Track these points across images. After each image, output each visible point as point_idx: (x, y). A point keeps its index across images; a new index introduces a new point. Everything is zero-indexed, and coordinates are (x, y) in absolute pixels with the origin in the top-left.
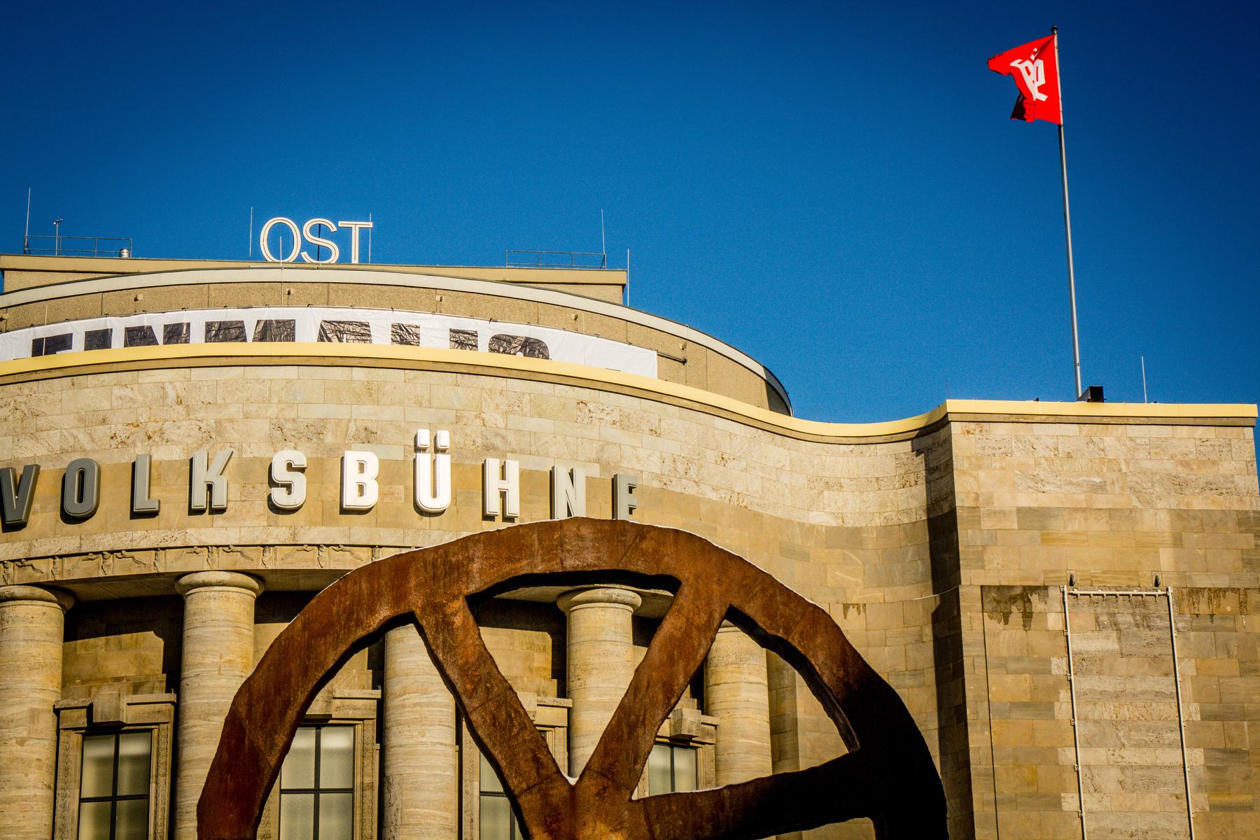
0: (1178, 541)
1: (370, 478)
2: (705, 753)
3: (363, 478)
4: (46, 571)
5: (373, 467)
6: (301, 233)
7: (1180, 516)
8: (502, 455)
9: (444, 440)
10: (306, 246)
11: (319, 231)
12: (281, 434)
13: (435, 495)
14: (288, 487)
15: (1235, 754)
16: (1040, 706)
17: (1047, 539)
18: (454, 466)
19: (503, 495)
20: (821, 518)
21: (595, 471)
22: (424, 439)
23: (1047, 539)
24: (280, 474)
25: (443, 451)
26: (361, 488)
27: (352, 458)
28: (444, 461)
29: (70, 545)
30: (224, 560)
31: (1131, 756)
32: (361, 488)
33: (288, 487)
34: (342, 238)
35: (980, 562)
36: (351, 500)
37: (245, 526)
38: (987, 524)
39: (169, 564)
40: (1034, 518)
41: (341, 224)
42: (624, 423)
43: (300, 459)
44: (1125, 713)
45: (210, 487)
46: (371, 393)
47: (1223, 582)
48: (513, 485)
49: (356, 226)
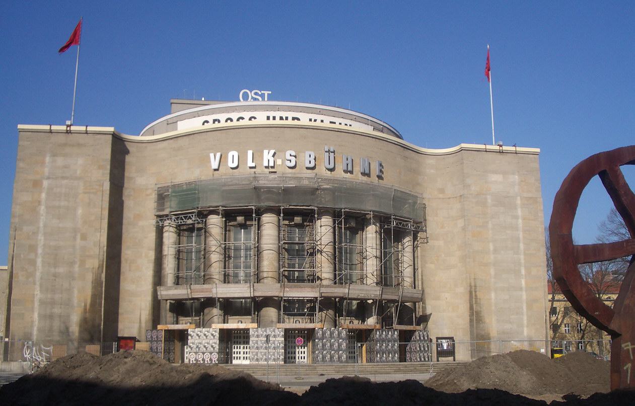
1: (312, 159)
6: (251, 94)
10: (252, 98)
11: (256, 94)
13: (329, 164)
14: (290, 161)
34: (262, 96)
41: (262, 92)
43: (293, 153)
45: (269, 160)
49: (266, 93)
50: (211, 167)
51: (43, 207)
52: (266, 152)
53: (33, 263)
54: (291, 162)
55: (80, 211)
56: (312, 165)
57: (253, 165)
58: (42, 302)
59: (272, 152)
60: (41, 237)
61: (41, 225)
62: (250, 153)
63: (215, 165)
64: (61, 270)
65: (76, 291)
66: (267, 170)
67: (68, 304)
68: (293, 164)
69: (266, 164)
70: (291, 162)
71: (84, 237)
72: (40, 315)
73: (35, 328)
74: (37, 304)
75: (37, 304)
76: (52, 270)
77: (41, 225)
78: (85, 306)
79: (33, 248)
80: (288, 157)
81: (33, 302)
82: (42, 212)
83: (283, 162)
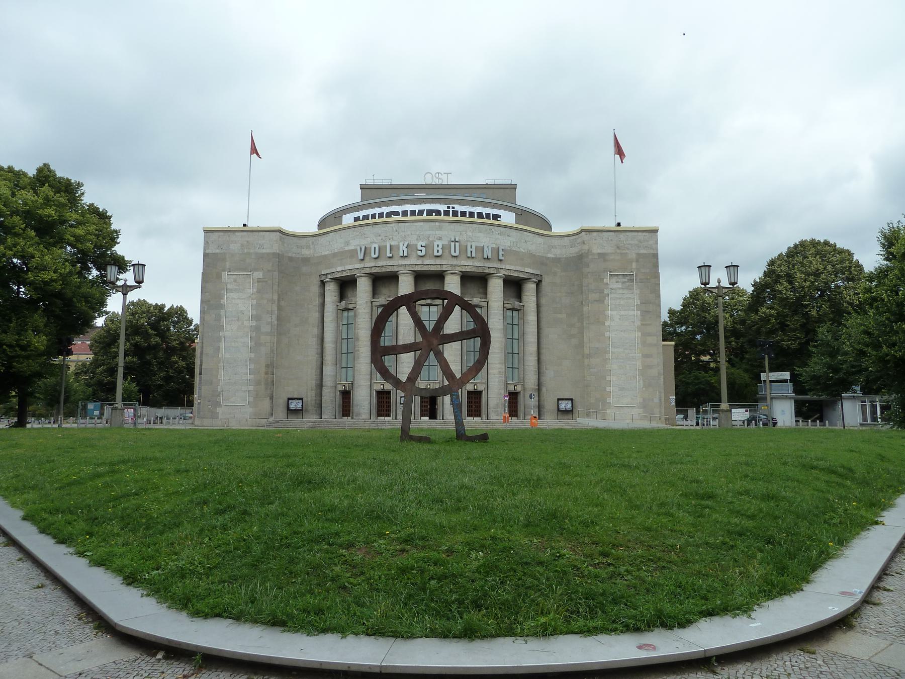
0: (637, 261)
2: (521, 312)
4: (368, 271)
5: (440, 246)
7: (638, 254)
12: (419, 238)
15: (648, 312)
16: (601, 301)
17: (605, 260)
20: (549, 255)
21: (494, 246)
23: (605, 260)
29: (372, 264)
30: (408, 268)
31: (623, 312)
35: (588, 266)
36: (436, 254)
37: (412, 261)
38: (590, 257)
39: (396, 269)
40: (602, 256)
42: (501, 234)
44: (622, 302)
46: (440, 228)
47: (648, 271)
48: (474, 250)
56: (439, 254)
68: (423, 253)
80: (420, 248)
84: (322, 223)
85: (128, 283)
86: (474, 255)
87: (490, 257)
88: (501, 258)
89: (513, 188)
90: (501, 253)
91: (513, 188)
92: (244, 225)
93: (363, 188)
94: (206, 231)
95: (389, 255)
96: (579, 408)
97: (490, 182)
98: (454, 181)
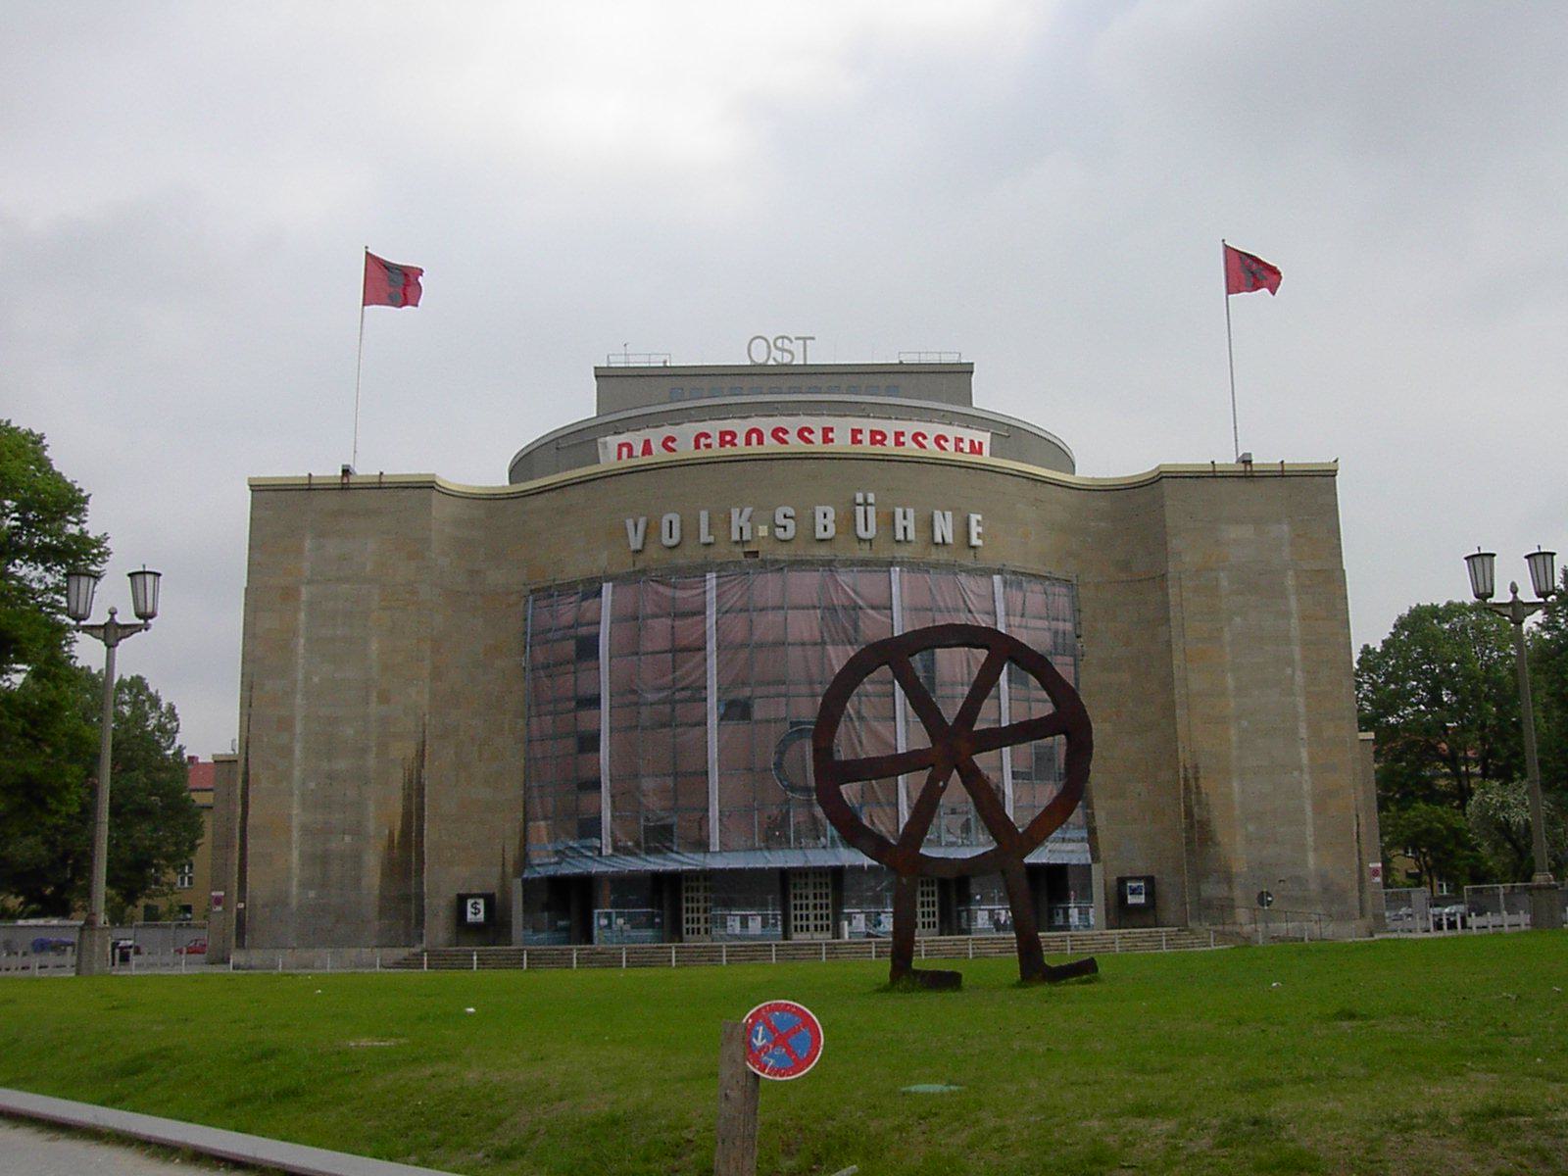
1: (830, 522)
3: (826, 522)
5: (831, 516)
8: (904, 506)
9: (871, 499)
13: (866, 529)
14: (785, 527)
18: (877, 513)
19: (905, 528)
22: (860, 499)
24: (780, 520)
25: (871, 504)
26: (825, 528)
27: (819, 511)
28: (871, 510)
32: (825, 528)
33: (785, 527)
36: (820, 534)
43: (791, 512)
45: (741, 529)
50: (629, 546)
51: (302, 641)
52: (735, 513)
53: (287, 752)
54: (785, 530)
55: (374, 646)
56: (831, 532)
57: (711, 539)
58: (305, 829)
59: (747, 511)
60: (299, 699)
61: (300, 676)
62: (704, 516)
63: (636, 543)
64: (342, 765)
65: (372, 808)
66: (738, 549)
67: (357, 831)
68: (790, 533)
69: (736, 536)
70: (785, 530)
71: (384, 698)
72: (302, 854)
73: (295, 882)
74: (295, 834)
75: (295, 834)
76: (325, 766)
77: (300, 676)
78: (391, 834)
79: (285, 724)
81: (289, 830)
82: (301, 650)
83: (772, 533)
84: (522, 466)
85: (119, 619)
86: (911, 536)
87: (949, 539)
88: (975, 541)
89: (965, 371)
90: (975, 529)
91: (965, 371)
92: (346, 472)
93: (602, 375)
94: (258, 489)
95: (705, 538)
96: (1170, 908)
97: (907, 359)
98: (819, 356)
